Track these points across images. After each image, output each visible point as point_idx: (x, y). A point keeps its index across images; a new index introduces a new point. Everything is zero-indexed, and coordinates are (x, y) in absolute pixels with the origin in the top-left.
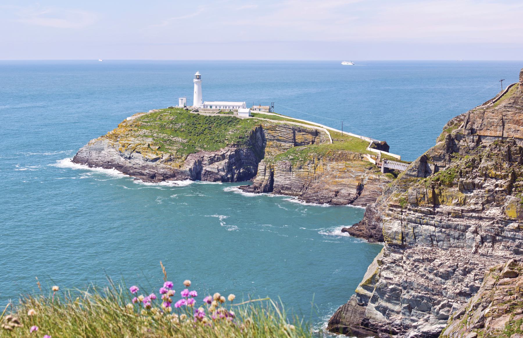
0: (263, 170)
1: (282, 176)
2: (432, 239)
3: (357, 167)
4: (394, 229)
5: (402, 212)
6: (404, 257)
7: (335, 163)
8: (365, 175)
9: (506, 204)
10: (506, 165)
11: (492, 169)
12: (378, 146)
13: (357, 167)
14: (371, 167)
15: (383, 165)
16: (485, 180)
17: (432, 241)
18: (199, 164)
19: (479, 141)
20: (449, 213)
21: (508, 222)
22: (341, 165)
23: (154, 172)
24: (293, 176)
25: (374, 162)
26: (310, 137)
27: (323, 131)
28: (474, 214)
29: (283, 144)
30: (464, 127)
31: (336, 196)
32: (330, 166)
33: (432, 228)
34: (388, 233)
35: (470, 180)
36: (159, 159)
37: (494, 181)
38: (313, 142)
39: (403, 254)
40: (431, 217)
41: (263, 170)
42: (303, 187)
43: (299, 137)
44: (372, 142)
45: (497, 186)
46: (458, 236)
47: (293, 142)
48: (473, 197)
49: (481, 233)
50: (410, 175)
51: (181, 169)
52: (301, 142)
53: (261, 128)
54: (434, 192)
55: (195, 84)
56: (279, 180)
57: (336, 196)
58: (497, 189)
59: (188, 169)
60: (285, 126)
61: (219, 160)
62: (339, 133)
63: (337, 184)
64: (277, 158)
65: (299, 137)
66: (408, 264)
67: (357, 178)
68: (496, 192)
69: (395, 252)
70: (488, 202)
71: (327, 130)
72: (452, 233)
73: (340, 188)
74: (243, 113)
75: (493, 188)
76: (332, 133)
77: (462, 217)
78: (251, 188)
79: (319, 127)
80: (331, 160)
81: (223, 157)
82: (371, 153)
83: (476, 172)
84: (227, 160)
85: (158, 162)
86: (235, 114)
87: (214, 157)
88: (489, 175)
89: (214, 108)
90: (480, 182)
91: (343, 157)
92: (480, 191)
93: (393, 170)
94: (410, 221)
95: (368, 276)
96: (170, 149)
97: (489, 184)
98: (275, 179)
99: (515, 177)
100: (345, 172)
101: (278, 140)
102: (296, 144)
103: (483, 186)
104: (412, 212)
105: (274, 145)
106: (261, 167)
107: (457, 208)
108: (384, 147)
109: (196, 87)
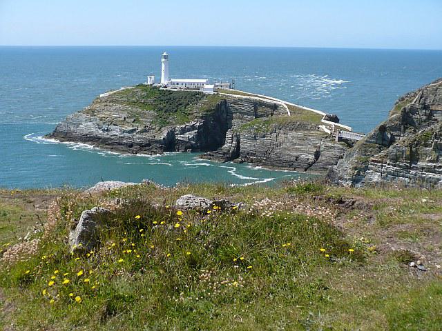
3: (314, 136)
4: (375, 180)
5: (382, 166)
14: (327, 136)
18: (172, 134)
20: (423, 168)
22: (301, 134)
24: (258, 143)
25: (329, 132)
26: (269, 110)
30: (417, 102)
31: (296, 160)
36: (135, 130)
38: (272, 115)
44: (324, 114)
50: (370, 142)
51: (156, 138)
53: (225, 102)
56: (245, 146)
57: (296, 160)
59: (162, 139)
60: (247, 101)
63: (297, 150)
64: (243, 128)
67: (314, 144)
71: (286, 105)
74: (208, 88)
80: (291, 130)
81: (193, 128)
84: (196, 131)
87: (185, 127)
91: (301, 127)
94: (389, 173)
98: (241, 146)
100: (304, 140)
106: (228, 136)
107: (430, 164)
108: (335, 119)
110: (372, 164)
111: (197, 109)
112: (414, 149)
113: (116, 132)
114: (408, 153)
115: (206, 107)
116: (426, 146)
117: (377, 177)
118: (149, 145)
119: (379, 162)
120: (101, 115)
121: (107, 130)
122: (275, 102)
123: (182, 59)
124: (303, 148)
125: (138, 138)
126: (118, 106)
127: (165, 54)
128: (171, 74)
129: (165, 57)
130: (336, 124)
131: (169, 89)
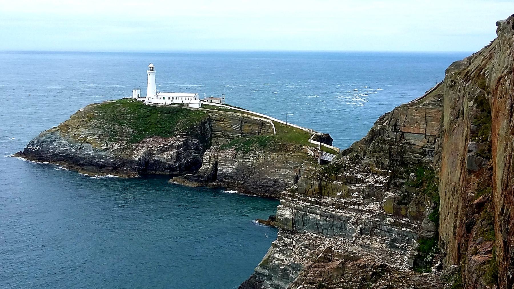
0: (208, 160)
1: (226, 165)
2: (318, 227)
3: (296, 158)
4: (286, 216)
5: (293, 200)
6: (294, 242)
7: (275, 154)
8: (303, 166)
10: (387, 162)
11: (372, 165)
12: (319, 138)
13: (296, 158)
15: (320, 157)
16: (366, 176)
17: (318, 228)
20: (333, 204)
22: (281, 155)
23: (105, 162)
25: (313, 154)
27: (268, 123)
28: (356, 207)
31: (274, 185)
32: (270, 156)
33: (318, 217)
34: (281, 219)
35: (353, 175)
36: (109, 148)
39: (293, 239)
40: (318, 207)
41: (208, 160)
42: (245, 176)
45: (377, 182)
46: (340, 226)
47: (240, 133)
52: (248, 133)
53: (210, 119)
54: (320, 185)
55: (149, 75)
56: (222, 168)
58: (377, 185)
61: (167, 150)
62: (284, 124)
65: (245, 128)
66: (297, 248)
68: (376, 187)
69: (286, 237)
70: (368, 196)
71: (272, 121)
72: (335, 222)
73: (278, 178)
74: (195, 104)
75: (373, 184)
77: (344, 208)
78: (195, 177)
79: (266, 118)
80: (272, 151)
81: (172, 147)
82: (311, 145)
83: (359, 168)
88: (370, 171)
89: (167, 98)
90: (361, 177)
92: (362, 186)
94: (300, 209)
95: (266, 257)
96: (120, 140)
97: (370, 180)
100: (284, 163)
103: (365, 181)
104: (301, 202)
105: (222, 135)
106: (206, 156)
107: (341, 200)
110: (285, 199)
112: (323, 183)
113: (90, 151)
114: (317, 187)
116: (337, 179)
117: (288, 212)
121: (80, 148)
122: (262, 119)
127: (151, 65)
129: (152, 69)
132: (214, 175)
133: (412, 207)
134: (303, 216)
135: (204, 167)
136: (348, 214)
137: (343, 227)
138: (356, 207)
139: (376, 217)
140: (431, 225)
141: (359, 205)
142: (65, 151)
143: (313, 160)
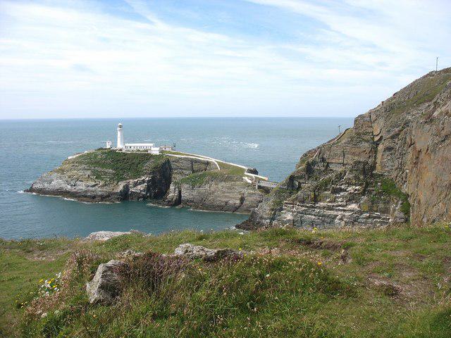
9: (362, 202)
10: (362, 177)
14: (248, 185)
18: (126, 187)
19: (327, 166)
20: (324, 208)
21: (361, 213)
22: (228, 184)
24: (195, 193)
25: (250, 182)
26: (203, 166)
28: (341, 208)
29: (184, 171)
35: (338, 187)
37: (354, 187)
43: (196, 167)
48: (340, 197)
49: (345, 220)
53: (169, 161)
60: (186, 159)
61: (140, 183)
63: (226, 196)
67: (240, 193)
74: (155, 151)
76: (219, 163)
77: (333, 210)
81: (143, 181)
82: (248, 176)
85: (96, 187)
86: (149, 152)
89: (132, 148)
93: (264, 187)
97: (351, 189)
99: (367, 185)
101: (180, 169)
102: (194, 172)
106: (172, 187)
109: (119, 133)
111: (149, 165)
112: (317, 193)
113: (82, 187)
115: (153, 165)
118: (108, 196)
119: (289, 204)
120: (69, 174)
123: (133, 128)
124: (231, 195)
125: (99, 191)
126: (83, 166)
127: (120, 124)
128: (126, 139)
129: (121, 127)
130: (256, 176)
131: (123, 151)
132: (179, 200)
133: (381, 206)
134: (301, 217)
135: (170, 195)
136: (336, 213)
137: (332, 222)
138: (341, 208)
139: (356, 213)
140: (402, 215)
141: (343, 206)
142: (62, 188)
143: (252, 186)
